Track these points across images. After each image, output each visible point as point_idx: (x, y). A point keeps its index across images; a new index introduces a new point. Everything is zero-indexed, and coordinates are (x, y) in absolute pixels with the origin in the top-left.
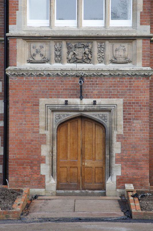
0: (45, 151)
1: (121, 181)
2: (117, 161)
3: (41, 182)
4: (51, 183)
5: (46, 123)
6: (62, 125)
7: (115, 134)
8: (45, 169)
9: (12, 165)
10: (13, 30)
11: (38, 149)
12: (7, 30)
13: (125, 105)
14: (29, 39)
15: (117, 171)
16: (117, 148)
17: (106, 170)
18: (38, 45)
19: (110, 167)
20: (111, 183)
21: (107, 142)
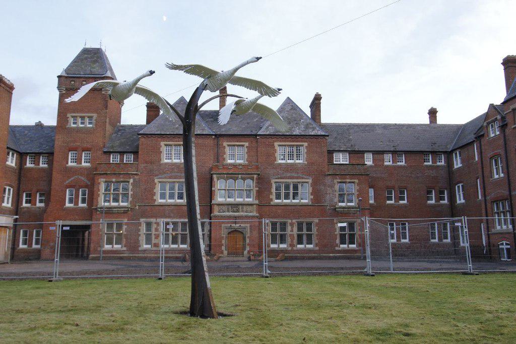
0: (223, 242)
1: (249, 252)
2: (248, 245)
3: (222, 253)
4: (226, 252)
5: (224, 233)
6: (229, 233)
7: (247, 237)
8: (223, 248)
9: (212, 247)
10: (213, 202)
11: (221, 242)
12: (211, 202)
13: (250, 226)
14: (218, 205)
15: (248, 248)
16: (248, 241)
17: (244, 248)
18: (221, 207)
19: (245, 247)
20: (246, 252)
21: (244, 239)
